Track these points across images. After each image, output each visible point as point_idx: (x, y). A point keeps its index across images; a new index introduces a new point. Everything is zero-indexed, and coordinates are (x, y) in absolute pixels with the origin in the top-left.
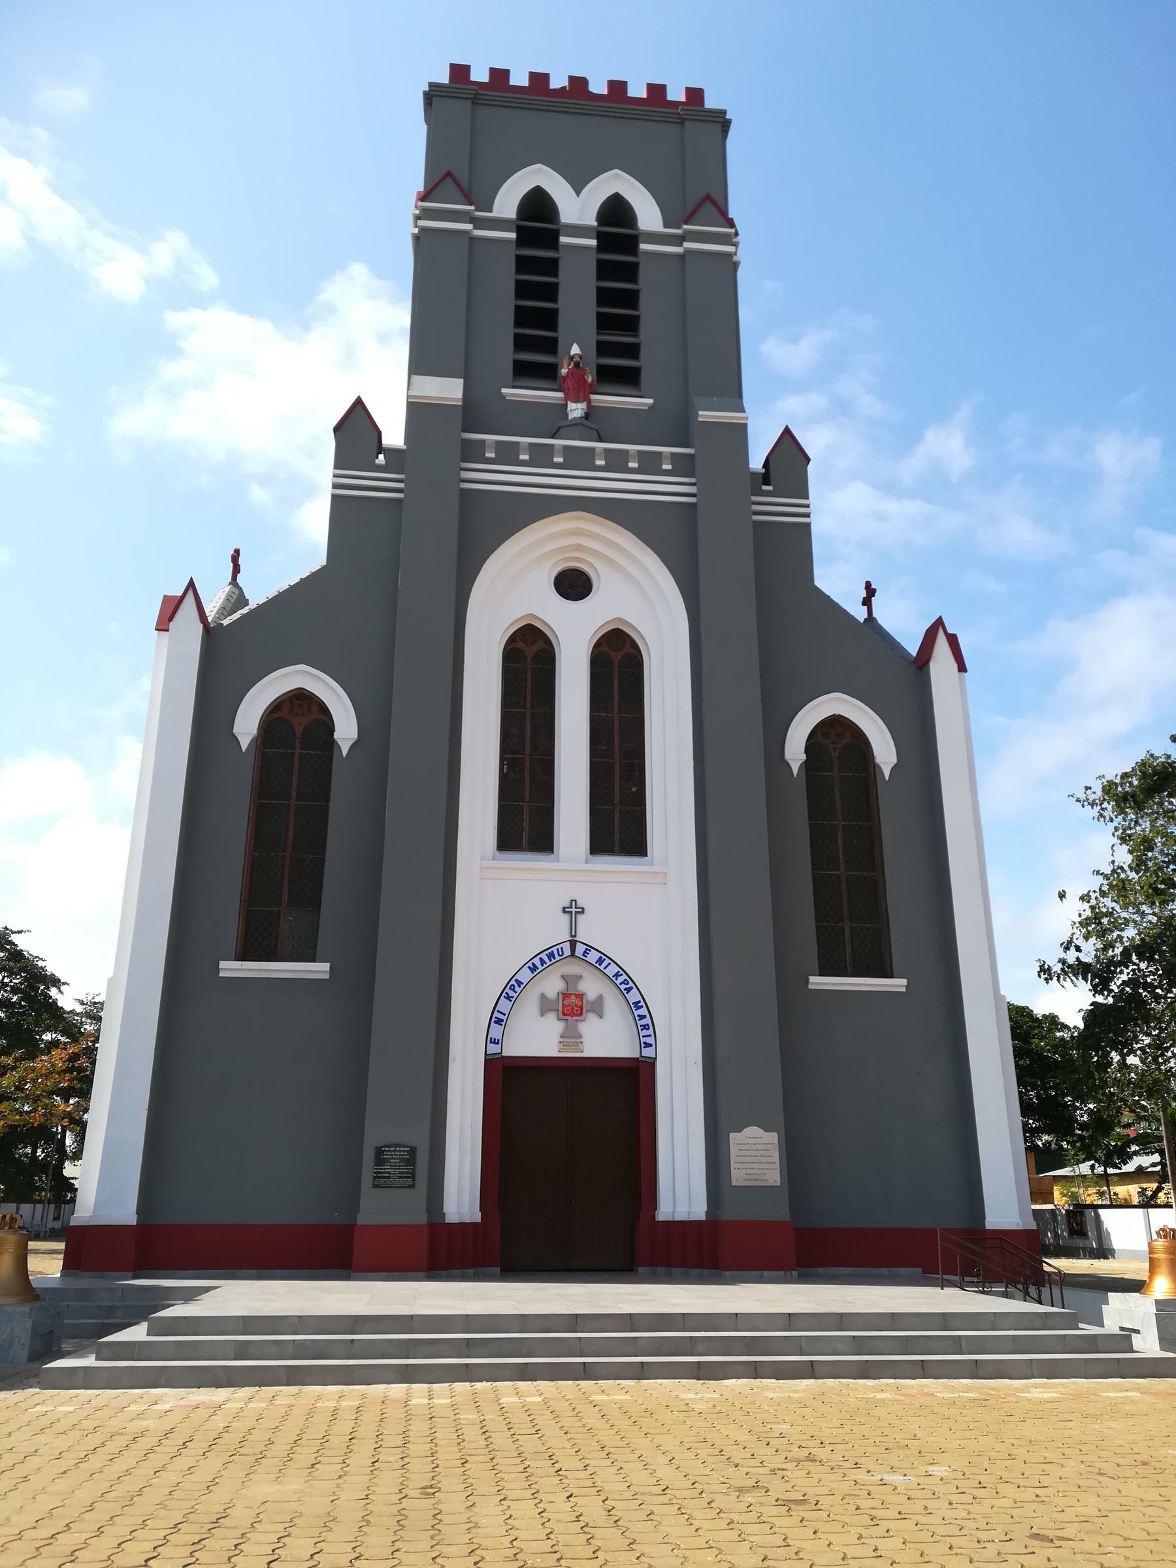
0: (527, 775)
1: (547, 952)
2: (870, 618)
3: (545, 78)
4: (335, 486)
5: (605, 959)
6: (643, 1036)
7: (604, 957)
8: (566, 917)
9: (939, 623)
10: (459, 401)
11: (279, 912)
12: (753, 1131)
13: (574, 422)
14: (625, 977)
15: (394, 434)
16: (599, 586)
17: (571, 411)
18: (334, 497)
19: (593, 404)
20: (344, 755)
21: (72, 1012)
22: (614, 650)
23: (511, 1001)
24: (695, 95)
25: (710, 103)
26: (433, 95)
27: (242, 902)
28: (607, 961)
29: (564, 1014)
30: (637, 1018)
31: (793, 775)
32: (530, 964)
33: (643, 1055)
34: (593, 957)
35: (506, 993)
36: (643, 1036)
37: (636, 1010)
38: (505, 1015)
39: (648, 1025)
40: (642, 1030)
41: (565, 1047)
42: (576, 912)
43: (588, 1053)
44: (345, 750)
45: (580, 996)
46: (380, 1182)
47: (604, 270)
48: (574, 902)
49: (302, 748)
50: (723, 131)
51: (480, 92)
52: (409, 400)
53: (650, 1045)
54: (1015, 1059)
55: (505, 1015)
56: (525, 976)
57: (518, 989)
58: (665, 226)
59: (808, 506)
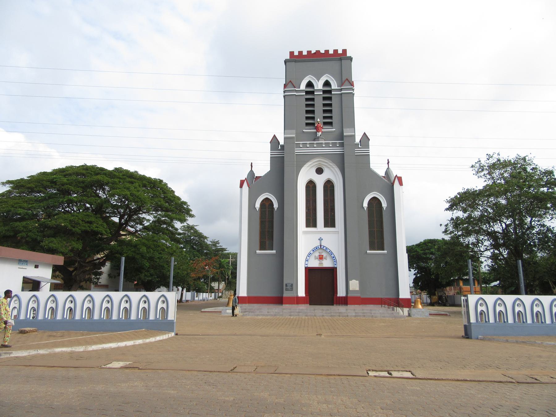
0: (311, 212)
2: (388, 168)
4: (271, 155)
8: (319, 241)
9: (396, 175)
12: (354, 281)
15: (282, 142)
18: (271, 157)
21: (210, 245)
24: (345, 51)
25: (348, 55)
26: (286, 62)
28: (327, 249)
34: (325, 248)
43: (324, 266)
45: (322, 256)
46: (287, 290)
50: (351, 60)
54: (409, 266)
56: (312, 252)
58: (338, 87)
59: (369, 150)
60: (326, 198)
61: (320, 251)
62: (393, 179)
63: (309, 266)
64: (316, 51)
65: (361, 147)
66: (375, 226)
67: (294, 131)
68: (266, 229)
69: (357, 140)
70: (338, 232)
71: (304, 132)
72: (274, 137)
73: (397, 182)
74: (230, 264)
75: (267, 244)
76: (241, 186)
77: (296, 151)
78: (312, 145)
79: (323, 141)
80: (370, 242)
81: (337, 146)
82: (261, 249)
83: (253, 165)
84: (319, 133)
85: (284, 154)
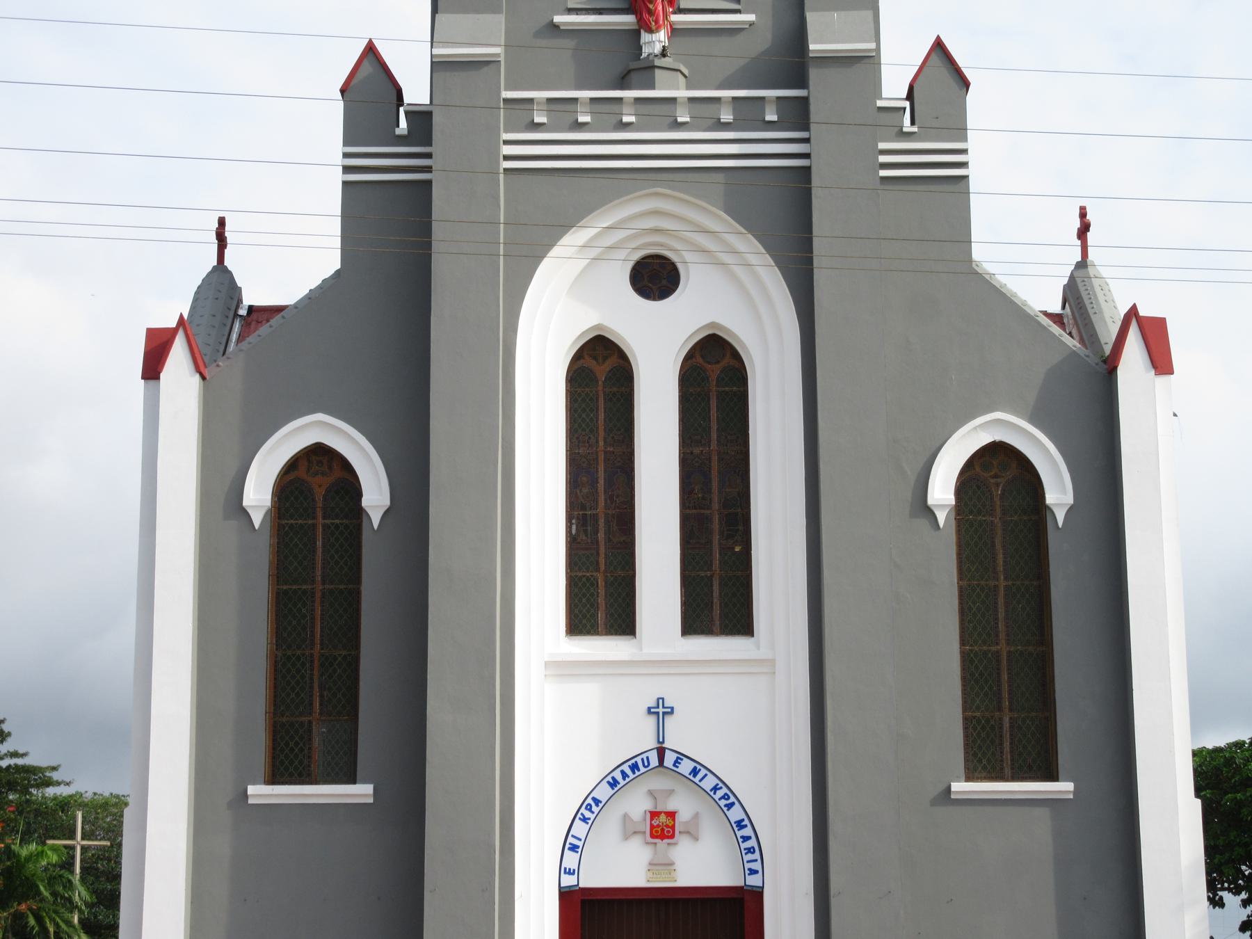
0: (601, 535)
1: (630, 763)
2: (1083, 264)
4: (347, 169)
5: (700, 770)
6: (748, 862)
7: (699, 767)
8: (652, 720)
9: (1133, 312)
11: (310, 722)
14: (725, 790)
15: (416, 91)
16: (688, 279)
18: (345, 183)
20: (376, 524)
22: (709, 363)
23: (587, 823)
27: (267, 715)
29: (652, 836)
30: (740, 840)
31: (938, 525)
32: (609, 779)
33: (747, 883)
34: (685, 767)
35: (582, 814)
36: (748, 862)
37: (739, 830)
38: (580, 840)
39: (753, 848)
40: (746, 854)
41: (655, 876)
42: (664, 713)
44: (376, 520)
45: (671, 815)
48: (661, 701)
49: (324, 518)
52: (434, 60)
53: (756, 872)
54: (1208, 873)
55: (580, 840)
57: (595, 809)
59: (964, 151)
60: (697, 451)
61: (659, 782)
62: (1114, 330)
63: (593, 878)
65: (915, 129)
66: (1001, 626)
67: (496, 23)
68: (313, 643)
69: (894, 86)
70: (771, 662)
71: (555, 27)
73: (1134, 355)
74: (72, 872)
75: (316, 741)
76: (153, 367)
78: (608, 113)
79: (678, 89)
80: (966, 720)
82: (276, 776)
84: (655, 37)
85: (428, 169)
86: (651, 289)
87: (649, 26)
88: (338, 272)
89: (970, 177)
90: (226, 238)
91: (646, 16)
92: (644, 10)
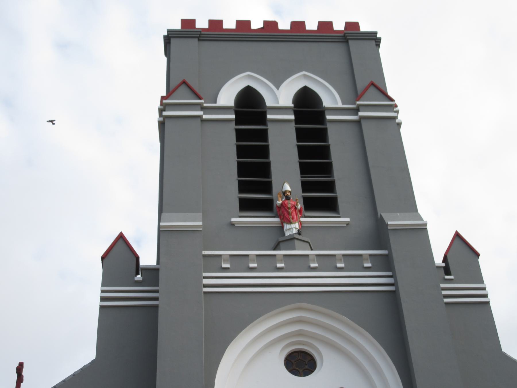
3: (248, 23)
4: (103, 299)
10: (201, 227)
13: (290, 238)
17: (287, 230)
18: (101, 307)
19: (303, 225)
47: (301, 135)
51: (203, 33)
52: (161, 230)
58: (343, 104)
64: (265, 22)
65: (451, 277)
71: (232, 224)
72: (121, 242)
77: (206, 281)
81: (366, 265)
83: (24, 373)
84: (293, 226)
86: (298, 371)
87: (288, 219)
88: (93, 361)
89: (490, 303)
90: (23, 376)
91: (286, 215)
92: (285, 213)
